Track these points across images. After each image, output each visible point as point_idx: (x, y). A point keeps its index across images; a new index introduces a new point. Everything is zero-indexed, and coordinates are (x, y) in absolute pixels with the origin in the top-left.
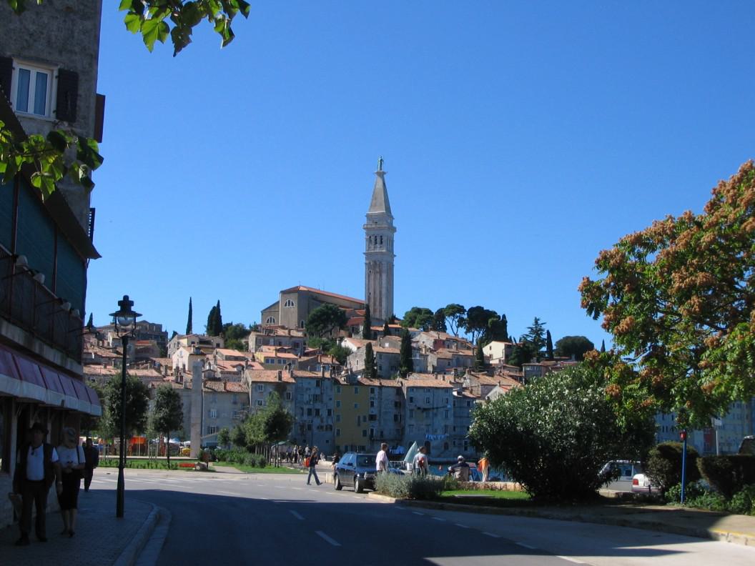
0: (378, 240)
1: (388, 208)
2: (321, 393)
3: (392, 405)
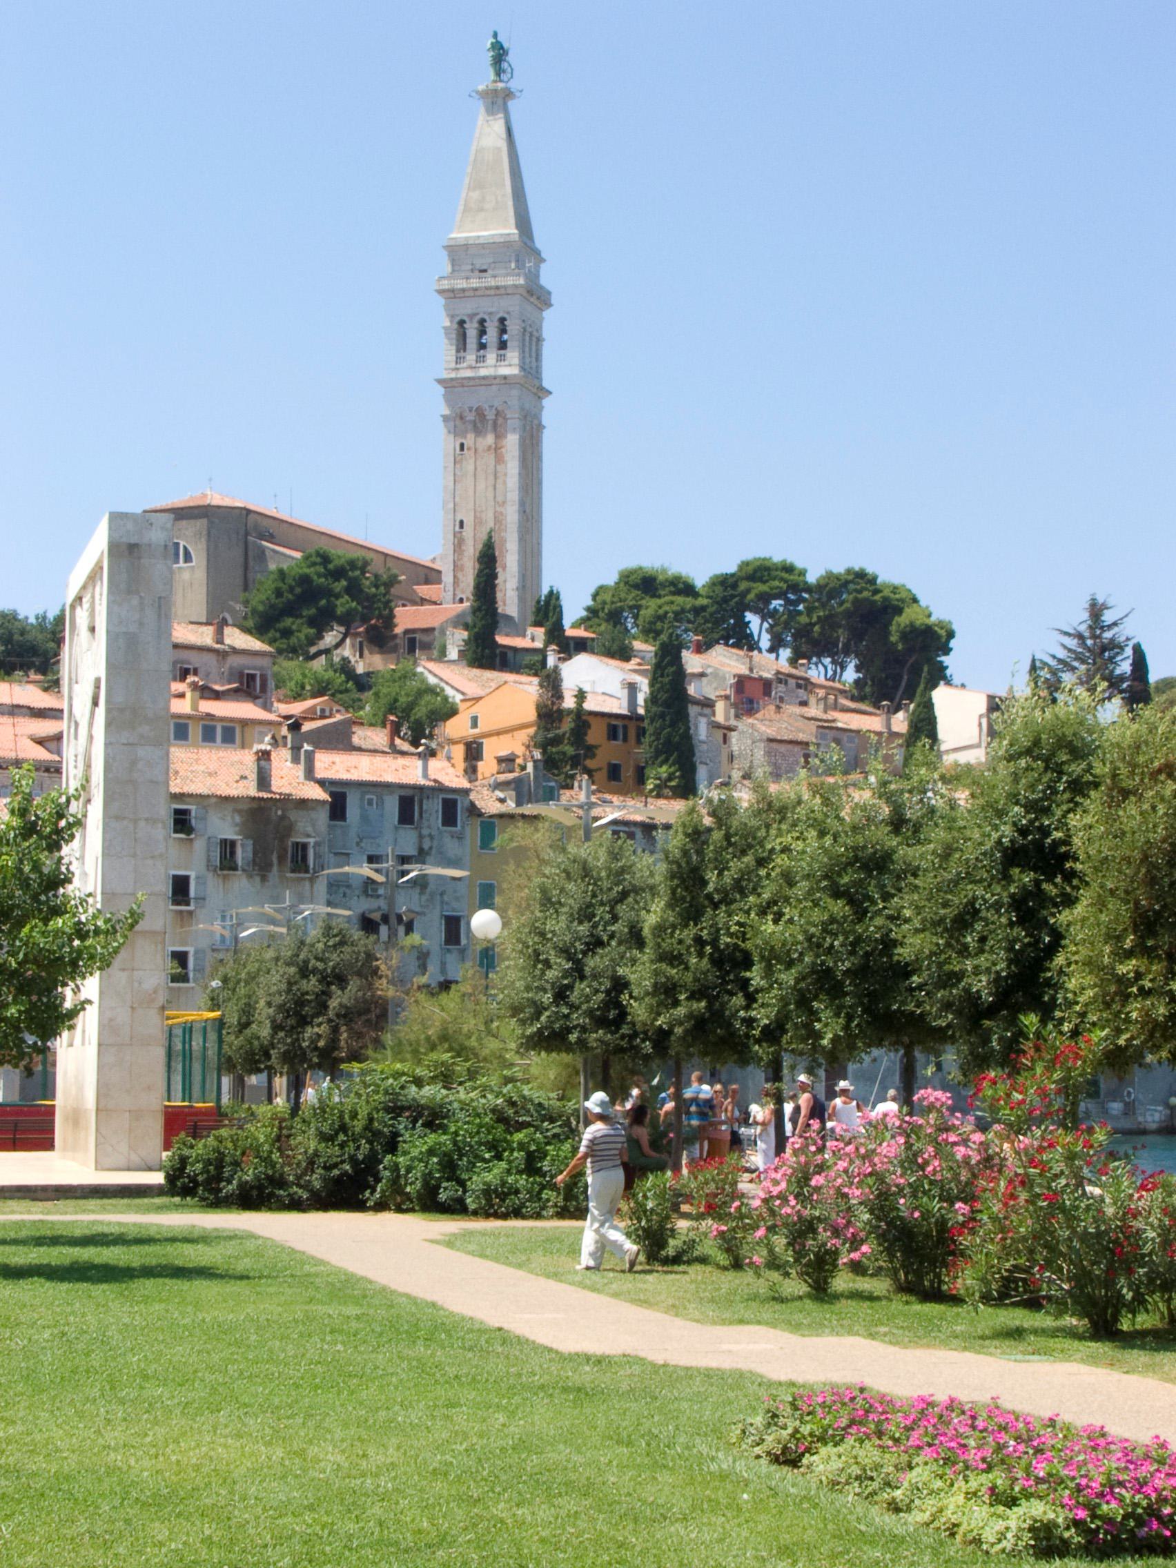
0: (491, 336)
1: (523, 222)
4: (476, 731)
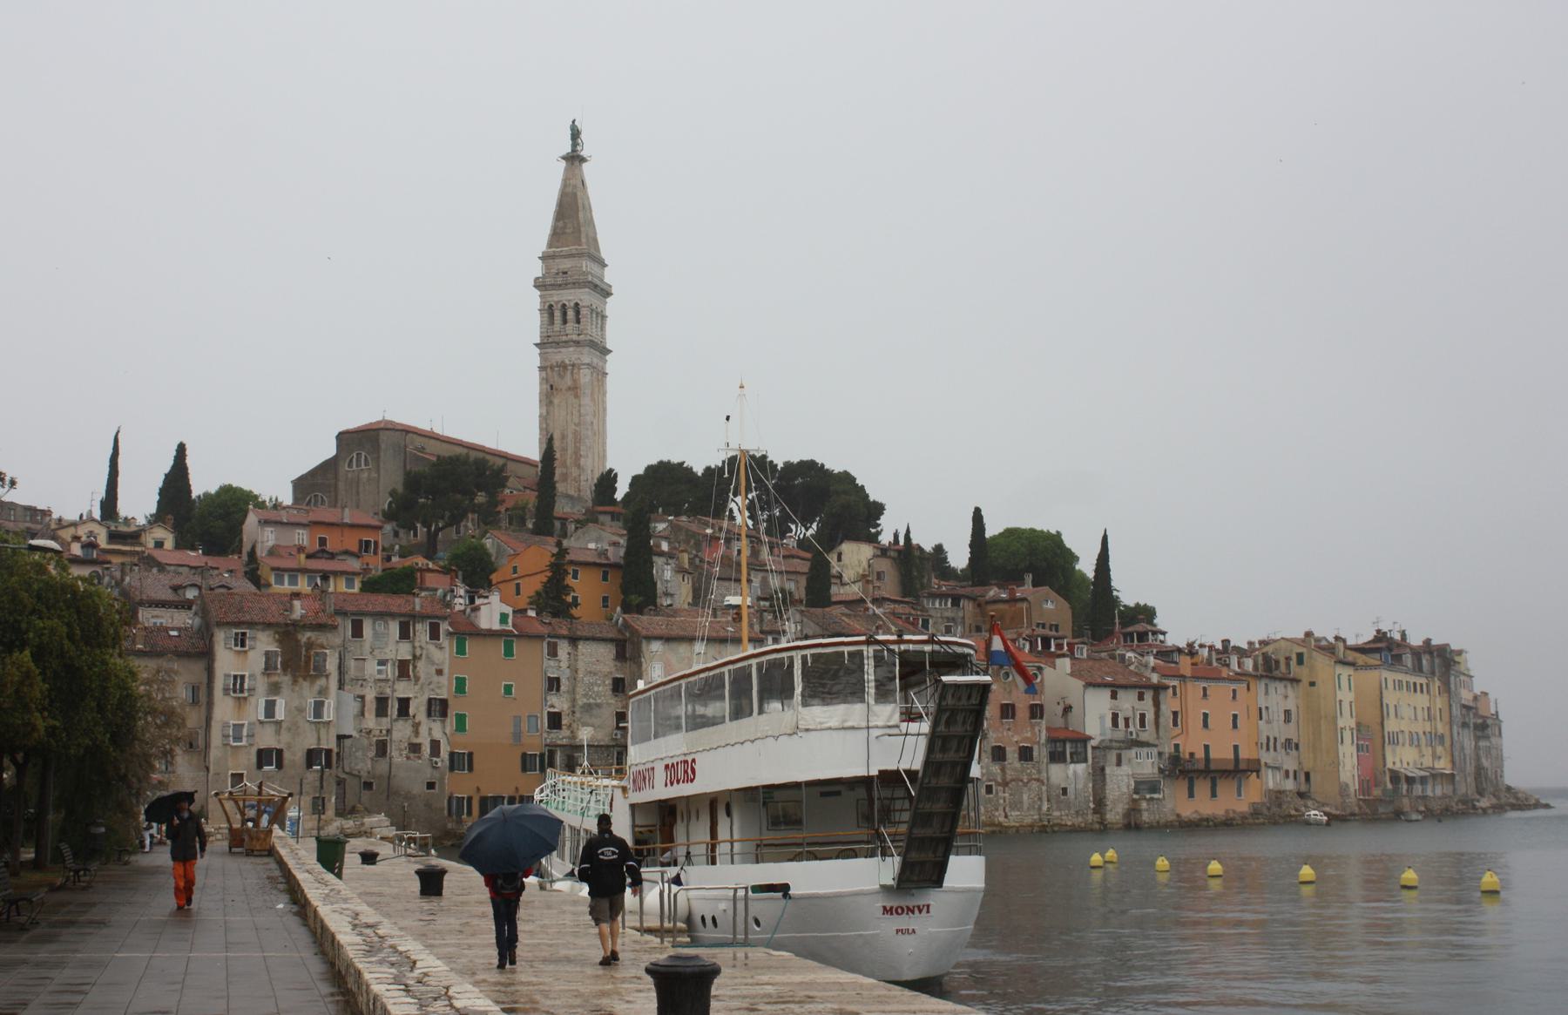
0: (571, 314)
2: (415, 657)
3: (604, 688)
4: (516, 575)
